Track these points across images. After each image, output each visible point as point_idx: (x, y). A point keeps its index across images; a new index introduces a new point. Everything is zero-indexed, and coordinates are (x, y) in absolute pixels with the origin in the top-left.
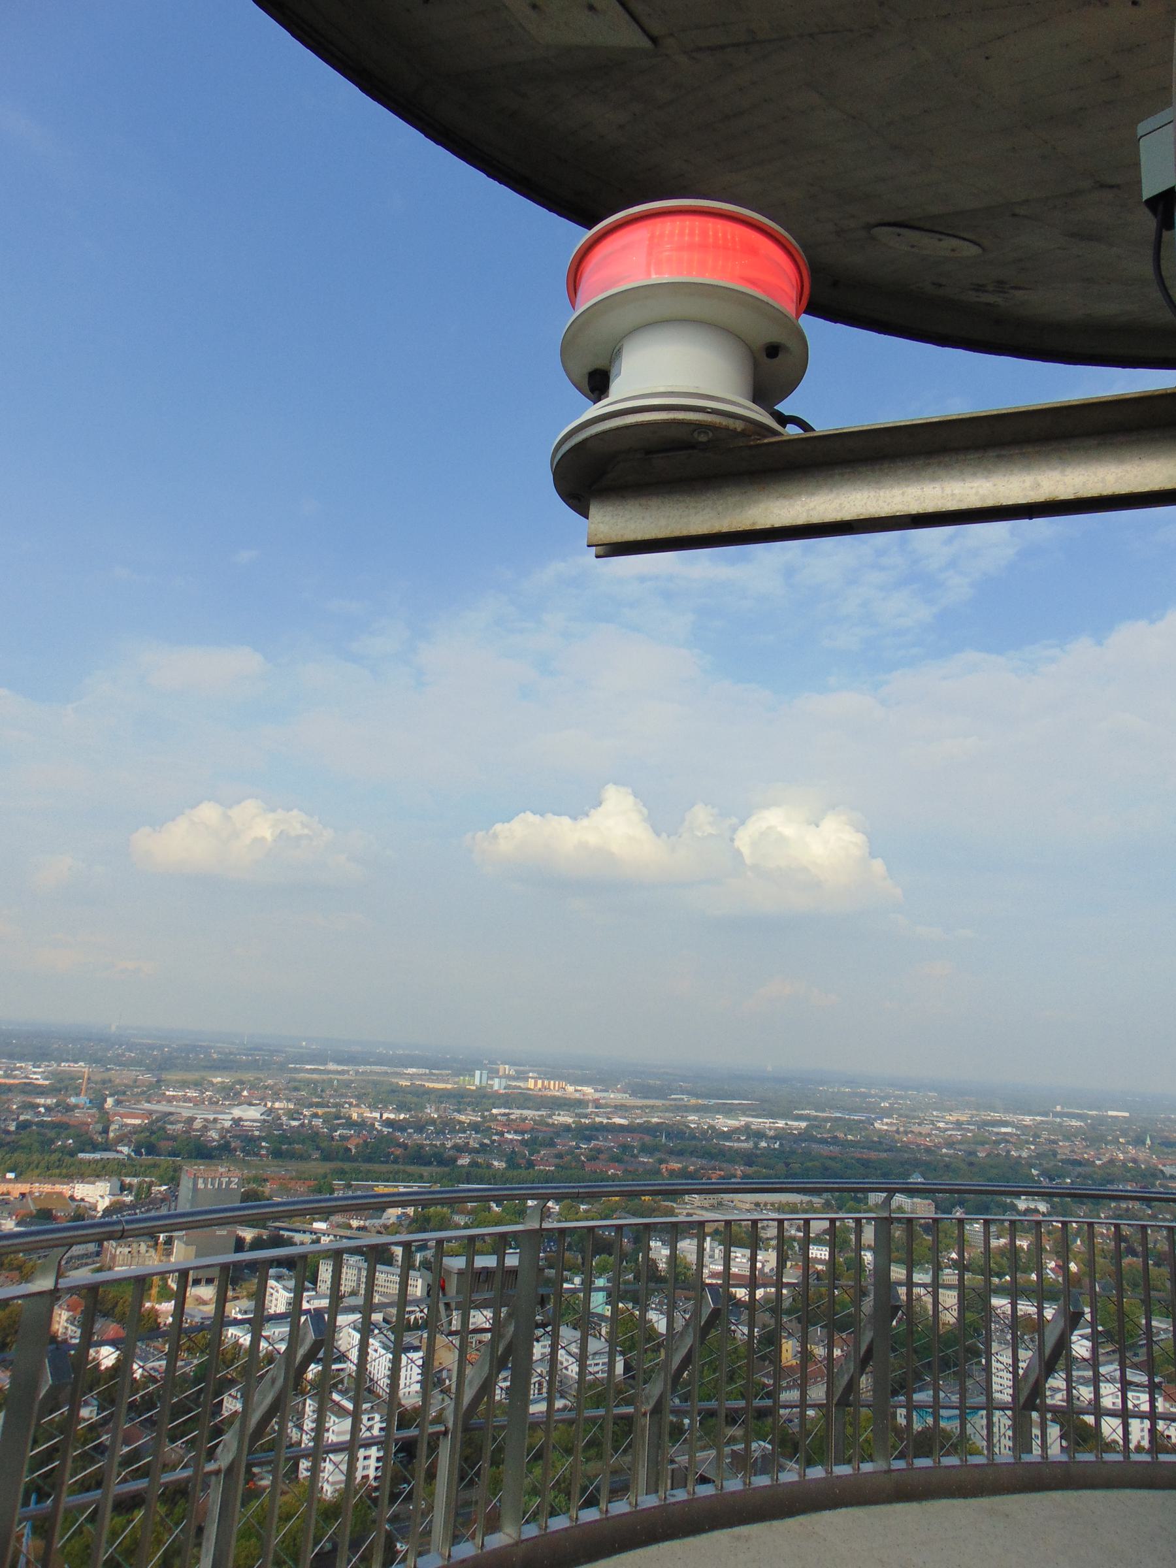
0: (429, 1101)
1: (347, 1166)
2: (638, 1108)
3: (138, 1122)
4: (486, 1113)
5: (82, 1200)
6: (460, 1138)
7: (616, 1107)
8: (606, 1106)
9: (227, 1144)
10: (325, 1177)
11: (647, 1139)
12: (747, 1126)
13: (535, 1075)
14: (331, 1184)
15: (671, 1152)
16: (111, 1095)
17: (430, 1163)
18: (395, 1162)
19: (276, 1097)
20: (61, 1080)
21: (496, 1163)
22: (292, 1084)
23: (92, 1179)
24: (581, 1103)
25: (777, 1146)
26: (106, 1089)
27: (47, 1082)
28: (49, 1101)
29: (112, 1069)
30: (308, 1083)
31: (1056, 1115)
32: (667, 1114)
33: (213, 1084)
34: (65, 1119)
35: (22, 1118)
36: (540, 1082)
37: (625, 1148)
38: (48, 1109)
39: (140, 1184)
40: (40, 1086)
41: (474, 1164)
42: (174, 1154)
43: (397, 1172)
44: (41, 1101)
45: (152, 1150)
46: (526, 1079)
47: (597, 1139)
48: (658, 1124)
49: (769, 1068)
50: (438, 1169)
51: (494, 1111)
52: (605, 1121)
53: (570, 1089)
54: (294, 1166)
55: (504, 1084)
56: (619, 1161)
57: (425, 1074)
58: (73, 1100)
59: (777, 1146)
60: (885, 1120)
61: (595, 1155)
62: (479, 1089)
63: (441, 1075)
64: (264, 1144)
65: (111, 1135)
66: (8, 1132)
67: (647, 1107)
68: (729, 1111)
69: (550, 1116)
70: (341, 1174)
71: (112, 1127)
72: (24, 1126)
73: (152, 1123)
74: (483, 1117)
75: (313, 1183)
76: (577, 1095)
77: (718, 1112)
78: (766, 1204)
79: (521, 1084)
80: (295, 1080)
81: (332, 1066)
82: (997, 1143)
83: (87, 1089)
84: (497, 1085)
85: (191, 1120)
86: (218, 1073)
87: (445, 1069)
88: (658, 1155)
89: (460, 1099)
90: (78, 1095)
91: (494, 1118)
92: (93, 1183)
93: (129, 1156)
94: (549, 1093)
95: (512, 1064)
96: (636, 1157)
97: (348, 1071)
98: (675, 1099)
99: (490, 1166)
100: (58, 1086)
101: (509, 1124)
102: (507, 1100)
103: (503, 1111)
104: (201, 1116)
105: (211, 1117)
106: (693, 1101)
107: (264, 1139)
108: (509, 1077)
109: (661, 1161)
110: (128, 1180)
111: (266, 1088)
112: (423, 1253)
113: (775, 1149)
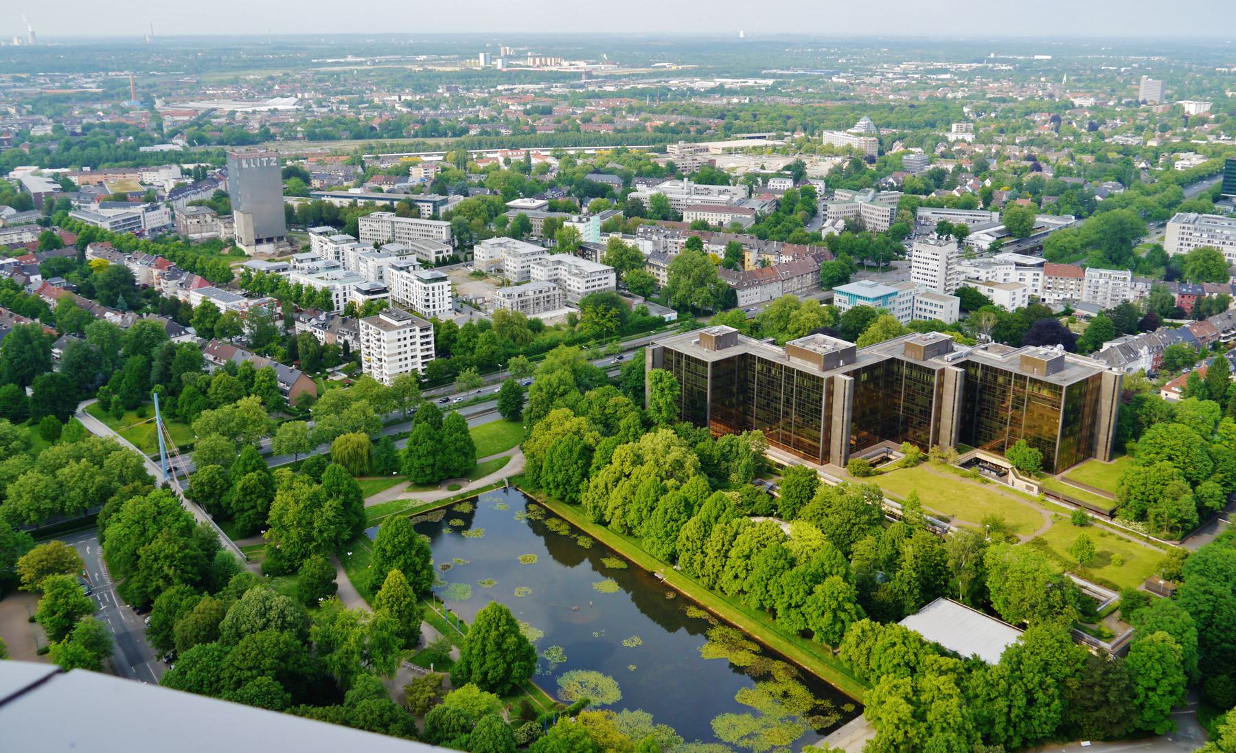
0: (440, 83)
1: (373, 142)
2: (625, 76)
3: (186, 118)
4: (492, 90)
5: (151, 184)
6: (471, 112)
7: (606, 77)
8: (597, 77)
9: (267, 131)
10: (356, 152)
11: (635, 103)
12: (722, 86)
13: (534, 54)
14: (360, 157)
15: (653, 112)
16: (159, 97)
17: (445, 135)
18: (416, 136)
19: (304, 89)
20: (112, 88)
21: (503, 131)
22: (316, 77)
23: (155, 167)
24: (577, 76)
25: (747, 101)
26: (154, 92)
27: (100, 90)
28: (105, 106)
29: (154, 75)
30: (332, 74)
32: (651, 81)
33: (246, 82)
34: (123, 120)
35: (84, 121)
36: (538, 60)
37: (614, 111)
38: (106, 113)
39: (196, 169)
40: (96, 93)
41: (484, 133)
42: (221, 142)
43: (418, 145)
44: (98, 106)
45: (202, 141)
46: (526, 58)
47: (591, 105)
48: (643, 89)
49: (742, 35)
50: (453, 139)
51: (500, 88)
52: (597, 90)
53: (565, 64)
54: (328, 146)
55: (506, 64)
56: (611, 122)
57: (435, 60)
58: (126, 104)
59: (747, 101)
60: (842, 74)
61: (587, 120)
62: (484, 69)
63: (450, 59)
64: (299, 129)
65: (165, 130)
66: (74, 134)
67: (633, 75)
68: (705, 75)
69: (549, 89)
70: (370, 149)
71: (164, 125)
72: (87, 128)
73: (200, 118)
74: (489, 93)
75: (345, 158)
76: (572, 69)
77: (696, 76)
78: (736, 149)
79: (521, 63)
80: (318, 73)
81: (350, 59)
83: (135, 93)
84: (499, 64)
85: (233, 113)
86: (250, 72)
87: (453, 54)
88: (643, 115)
89: (469, 78)
90: (129, 98)
91: (499, 93)
92: (157, 171)
93: (184, 147)
94: (546, 69)
95: (512, 46)
96: (624, 117)
97: (366, 62)
98: (658, 67)
99: (498, 134)
100: (110, 92)
101: (513, 96)
102: (511, 77)
103: (506, 87)
104: (242, 108)
105: (250, 110)
106: (674, 68)
107: (299, 124)
108: (510, 57)
109: (646, 120)
110: (186, 166)
111: (294, 81)
112: (445, 207)
113: (745, 104)
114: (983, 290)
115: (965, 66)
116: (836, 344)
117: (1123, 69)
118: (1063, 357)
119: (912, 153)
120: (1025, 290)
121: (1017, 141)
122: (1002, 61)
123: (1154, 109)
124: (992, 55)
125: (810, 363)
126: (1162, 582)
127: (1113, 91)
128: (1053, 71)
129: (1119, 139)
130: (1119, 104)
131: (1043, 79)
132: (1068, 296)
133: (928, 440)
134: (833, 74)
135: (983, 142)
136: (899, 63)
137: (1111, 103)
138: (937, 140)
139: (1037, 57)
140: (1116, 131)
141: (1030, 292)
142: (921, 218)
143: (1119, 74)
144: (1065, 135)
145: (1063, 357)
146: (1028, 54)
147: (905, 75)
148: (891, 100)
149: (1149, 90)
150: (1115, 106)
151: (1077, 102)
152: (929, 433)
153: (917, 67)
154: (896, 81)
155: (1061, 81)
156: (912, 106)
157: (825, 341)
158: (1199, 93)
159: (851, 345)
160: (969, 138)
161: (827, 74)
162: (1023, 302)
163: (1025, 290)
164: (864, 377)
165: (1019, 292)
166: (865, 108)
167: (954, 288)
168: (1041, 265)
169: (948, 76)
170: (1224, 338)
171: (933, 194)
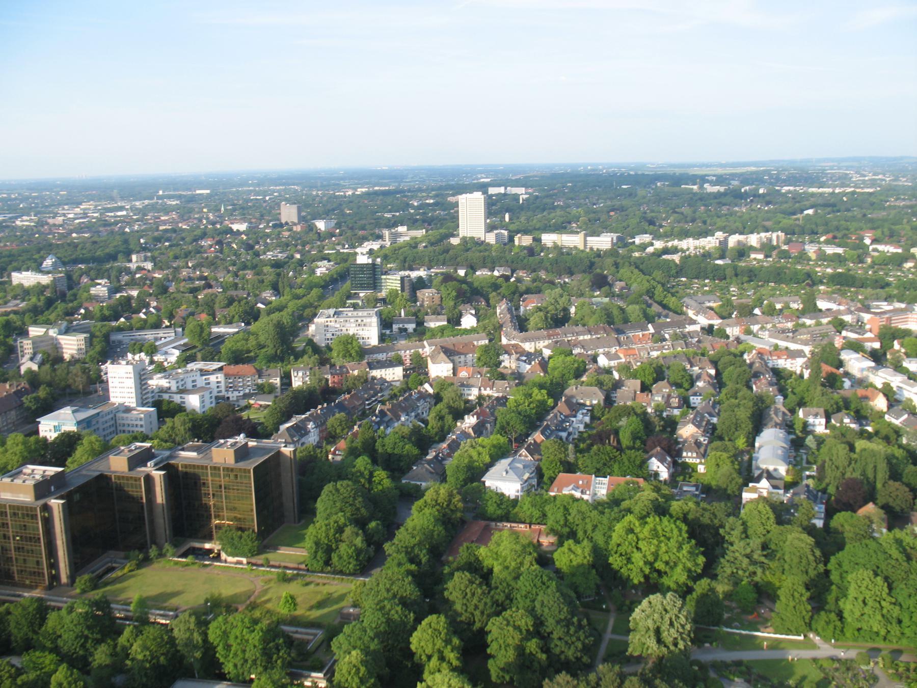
31: (159, 198)
60: (25, 218)
82: (116, 223)
114: (177, 399)
115: (138, 204)
116: (44, 472)
117: (267, 198)
118: (246, 444)
119: (99, 284)
120: (211, 393)
121: (190, 265)
122: (170, 197)
123: (295, 228)
124: (161, 193)
125: (21, 495)
126: (351, 610)
127: (262, 216)
128: (213, 202)
129: (269, 255)
130: (267, 227)
131: (205, 210)
132: (247, 391)
133: (146, 541)
134: (16, 218)
135: (161, 269)
136: (78, 204)
137: (261, 226)
138: (121, 271)
139: (198, 192)
140: (267, 249)
141: (215, 394)
142: (114, 342)
143: (265, 201)
144: (228, 256)
145: (246, 444)
146: (190, 190)
147: (85, 215)
148: (75, 238)
149: (288, 213)
150: (265, 228)
151: (235, 227)
152: (145, 536)
153: (96, 206)
154: (77, 221)
155: (220, 210)
156: (95, 242)
157: (33, 471)
158: (324, 214)
159: (60, 469)
160: (149, 266)
161: (11, 218)
162: (211, 403)
163: (211, 393)
164: (77, 497)
165: (207, 395)
166: (49, 248)
167: (150, 400)
168: (221, 369)
169: (124, 213)
170: (369, 404)
171: (122, 320)
